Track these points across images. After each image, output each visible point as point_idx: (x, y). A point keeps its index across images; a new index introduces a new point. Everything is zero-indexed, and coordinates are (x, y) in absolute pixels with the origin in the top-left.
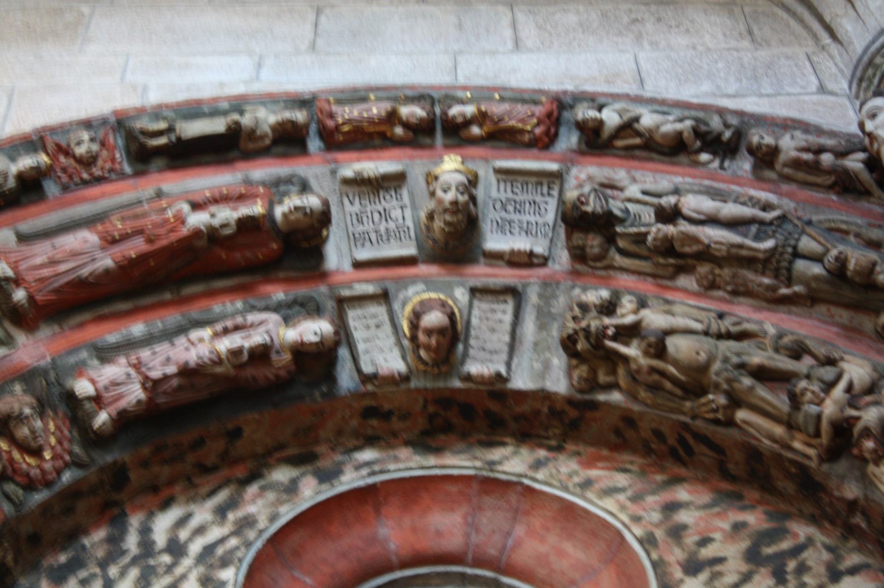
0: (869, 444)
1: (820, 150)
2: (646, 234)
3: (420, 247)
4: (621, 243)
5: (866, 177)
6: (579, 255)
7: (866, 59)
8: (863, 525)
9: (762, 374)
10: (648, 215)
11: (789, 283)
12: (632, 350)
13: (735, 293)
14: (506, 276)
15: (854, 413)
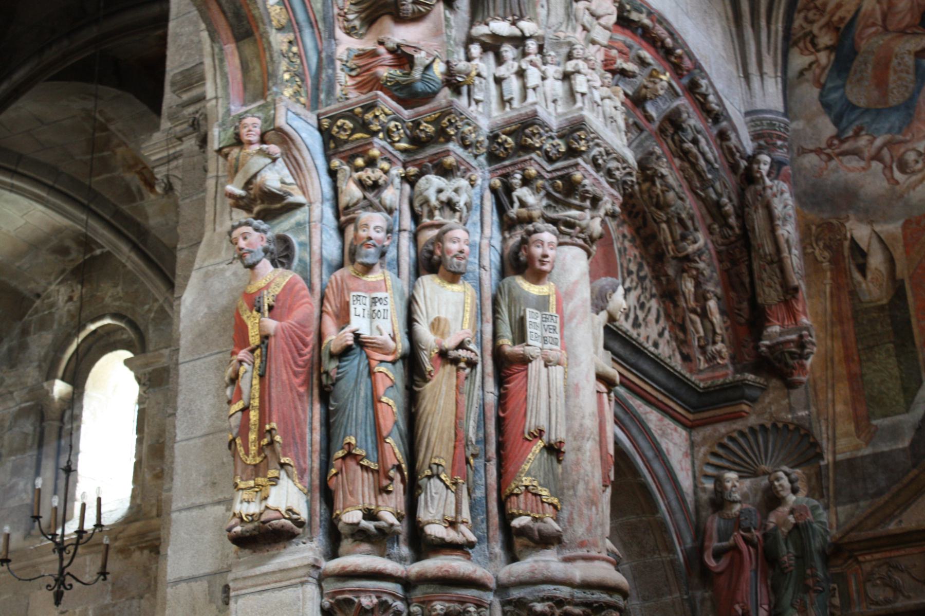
0: (694, 273)
1: (738, 151)
2: (685, 142)
3: (634, 93)
4: (676, 137)
5: (741, 171)
6: (662, 131)
7: (761, 116)
8: (664, 282)
9: (681, 221)
10: (690, 137)
11: (703, 190)
12: (658, 182)
13: (686, 178)
14: (643, 122)
15: (697, 259)
